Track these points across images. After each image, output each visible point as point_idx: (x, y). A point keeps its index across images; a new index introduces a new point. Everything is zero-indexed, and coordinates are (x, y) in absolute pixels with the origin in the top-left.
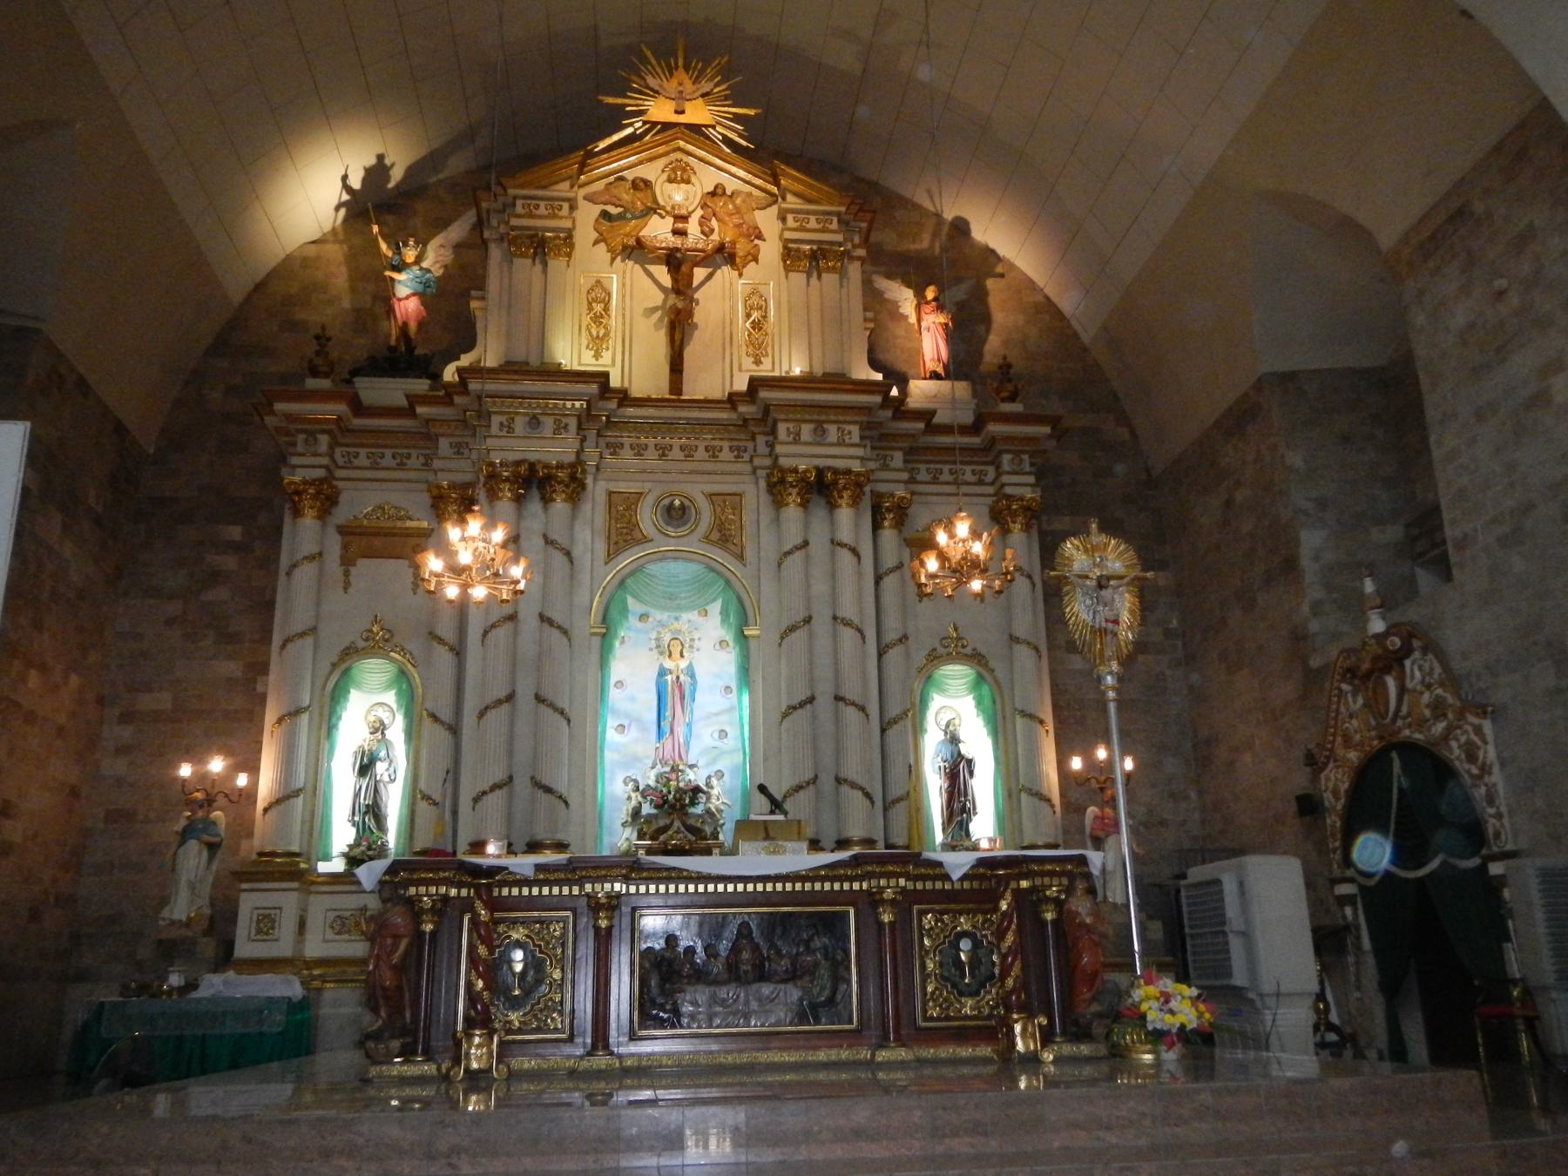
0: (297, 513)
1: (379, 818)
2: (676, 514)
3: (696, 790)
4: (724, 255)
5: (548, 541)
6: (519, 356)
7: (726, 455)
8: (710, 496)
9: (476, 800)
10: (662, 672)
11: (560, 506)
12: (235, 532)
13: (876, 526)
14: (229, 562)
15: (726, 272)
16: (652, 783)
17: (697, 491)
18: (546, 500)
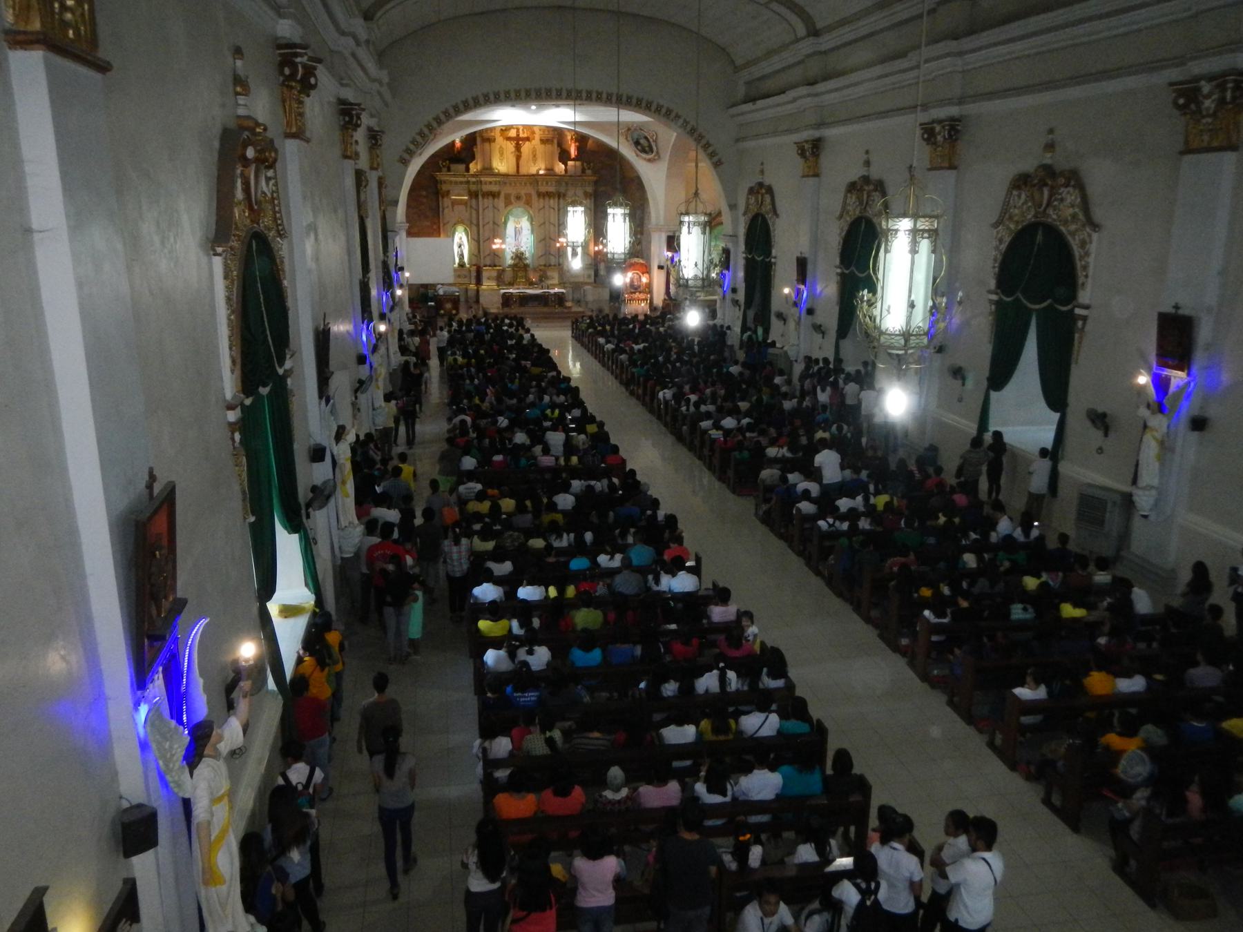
0: (443, 197)
1: (463, 257)
2: (518, 198)
3: (522, 254)
4: (528, 139)
5: (494, 207)
6: (486, 166)
7: (528, 184)
8: (526, 194)
9: (485, 257)
10: (516, 228)
11: (496, 200)
12: (424, 193)
13: (559, 199)
14: (425, 200)
15: (527, 143)
16: (514, 250)
17: (523, 192)
18: (494, 199)
